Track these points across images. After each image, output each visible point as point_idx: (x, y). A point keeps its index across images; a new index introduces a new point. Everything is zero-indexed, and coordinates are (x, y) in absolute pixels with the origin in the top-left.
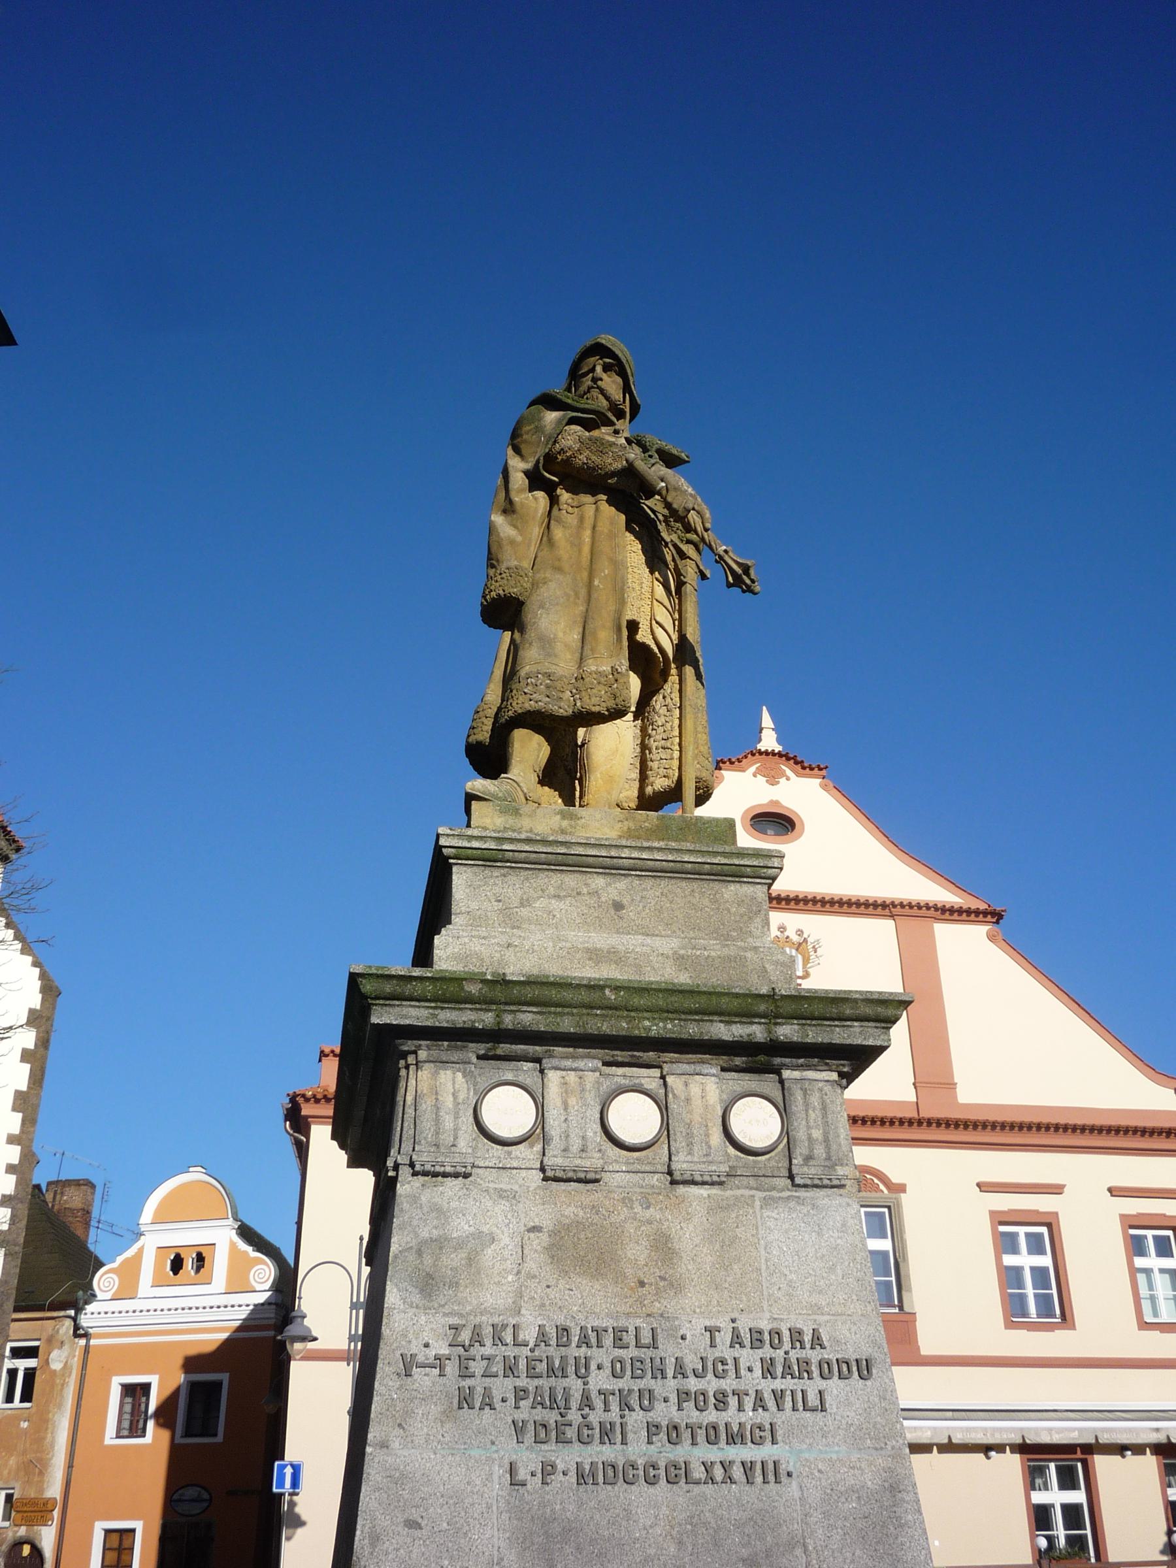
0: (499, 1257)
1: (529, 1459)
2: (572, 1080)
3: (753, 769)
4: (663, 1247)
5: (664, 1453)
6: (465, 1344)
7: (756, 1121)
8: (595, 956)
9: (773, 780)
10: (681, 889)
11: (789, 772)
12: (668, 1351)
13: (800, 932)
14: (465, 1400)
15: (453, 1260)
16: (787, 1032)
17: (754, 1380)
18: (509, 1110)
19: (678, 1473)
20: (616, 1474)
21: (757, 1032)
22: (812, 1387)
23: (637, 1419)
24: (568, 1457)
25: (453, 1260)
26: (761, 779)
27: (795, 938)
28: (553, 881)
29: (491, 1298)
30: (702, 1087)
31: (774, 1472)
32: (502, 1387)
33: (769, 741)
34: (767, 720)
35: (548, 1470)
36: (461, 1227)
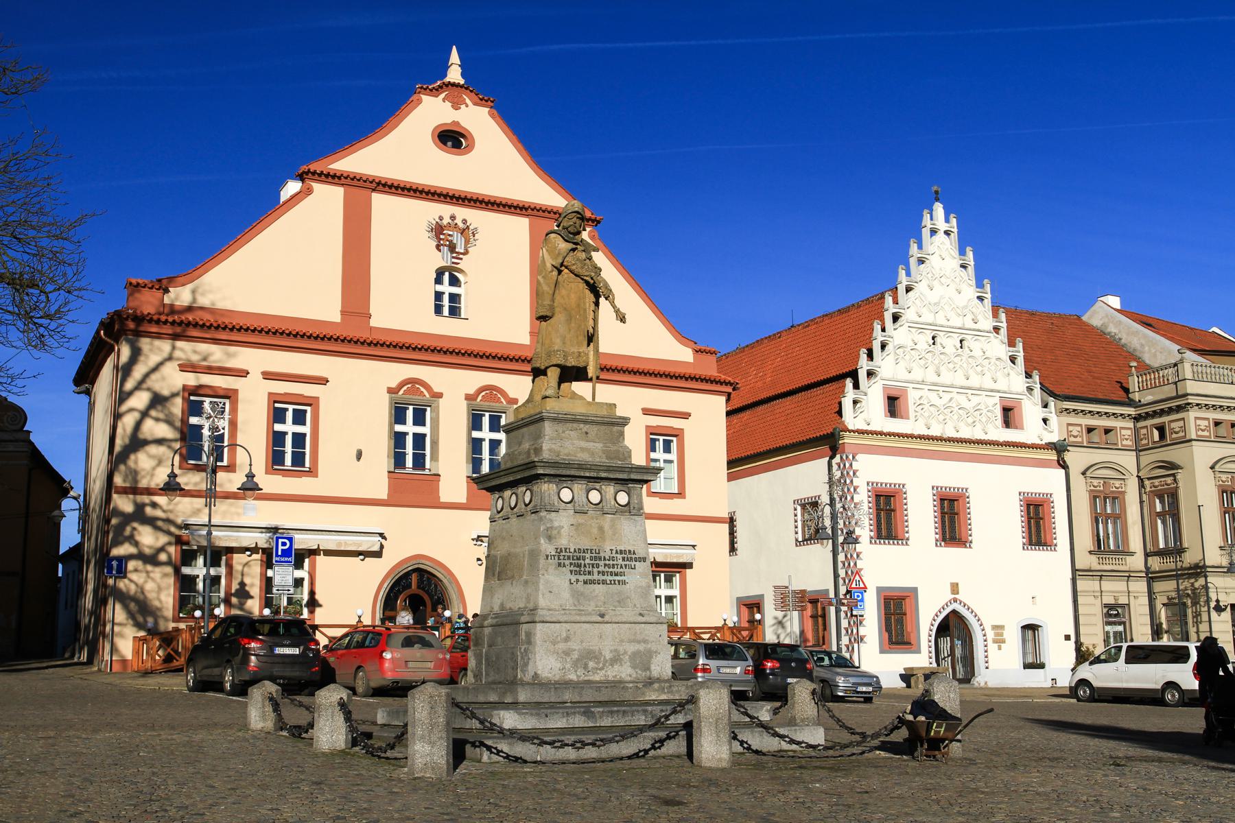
0: (564, 532)
1: (573, 578)
2: (579, 487)
3: (443, 95)
4: (601, 529)
5: (601, 577)
6: (559, 551)
7: (623, 498)
8: (583, 449)
9: (456, 107)
10: (603, 427)
11: (468, 101)
12: (602, 555)
13: (465, 221)
14: (559, 565)
15: (555, 532)
16: (633, 476)
17: (620, 562)
18: (566, 495)
19: (604, 582)
20: (592, 582)
21: (624, 476)
22: (633, 563)
23: (595, 570)
24: (582, 578)
25: (555, 532)
26: (448, 104)
27: (461, 225)
28: (569, 425)
29: (563, 542)
30: (610, 489)
31: (624, 583)
32: (567, 562)
33: (454, 74)
34: (455, 57)
35: (578, 581)
36: (556, 524)
